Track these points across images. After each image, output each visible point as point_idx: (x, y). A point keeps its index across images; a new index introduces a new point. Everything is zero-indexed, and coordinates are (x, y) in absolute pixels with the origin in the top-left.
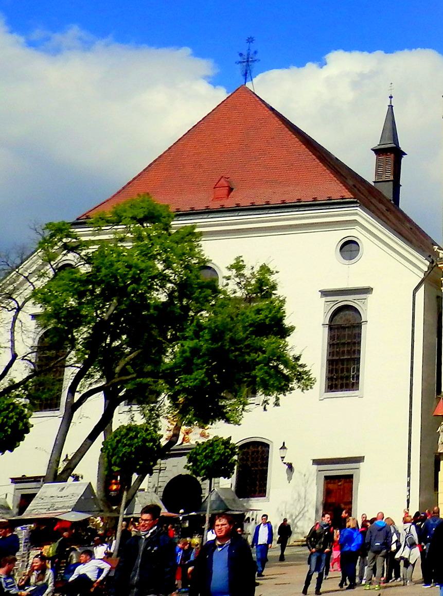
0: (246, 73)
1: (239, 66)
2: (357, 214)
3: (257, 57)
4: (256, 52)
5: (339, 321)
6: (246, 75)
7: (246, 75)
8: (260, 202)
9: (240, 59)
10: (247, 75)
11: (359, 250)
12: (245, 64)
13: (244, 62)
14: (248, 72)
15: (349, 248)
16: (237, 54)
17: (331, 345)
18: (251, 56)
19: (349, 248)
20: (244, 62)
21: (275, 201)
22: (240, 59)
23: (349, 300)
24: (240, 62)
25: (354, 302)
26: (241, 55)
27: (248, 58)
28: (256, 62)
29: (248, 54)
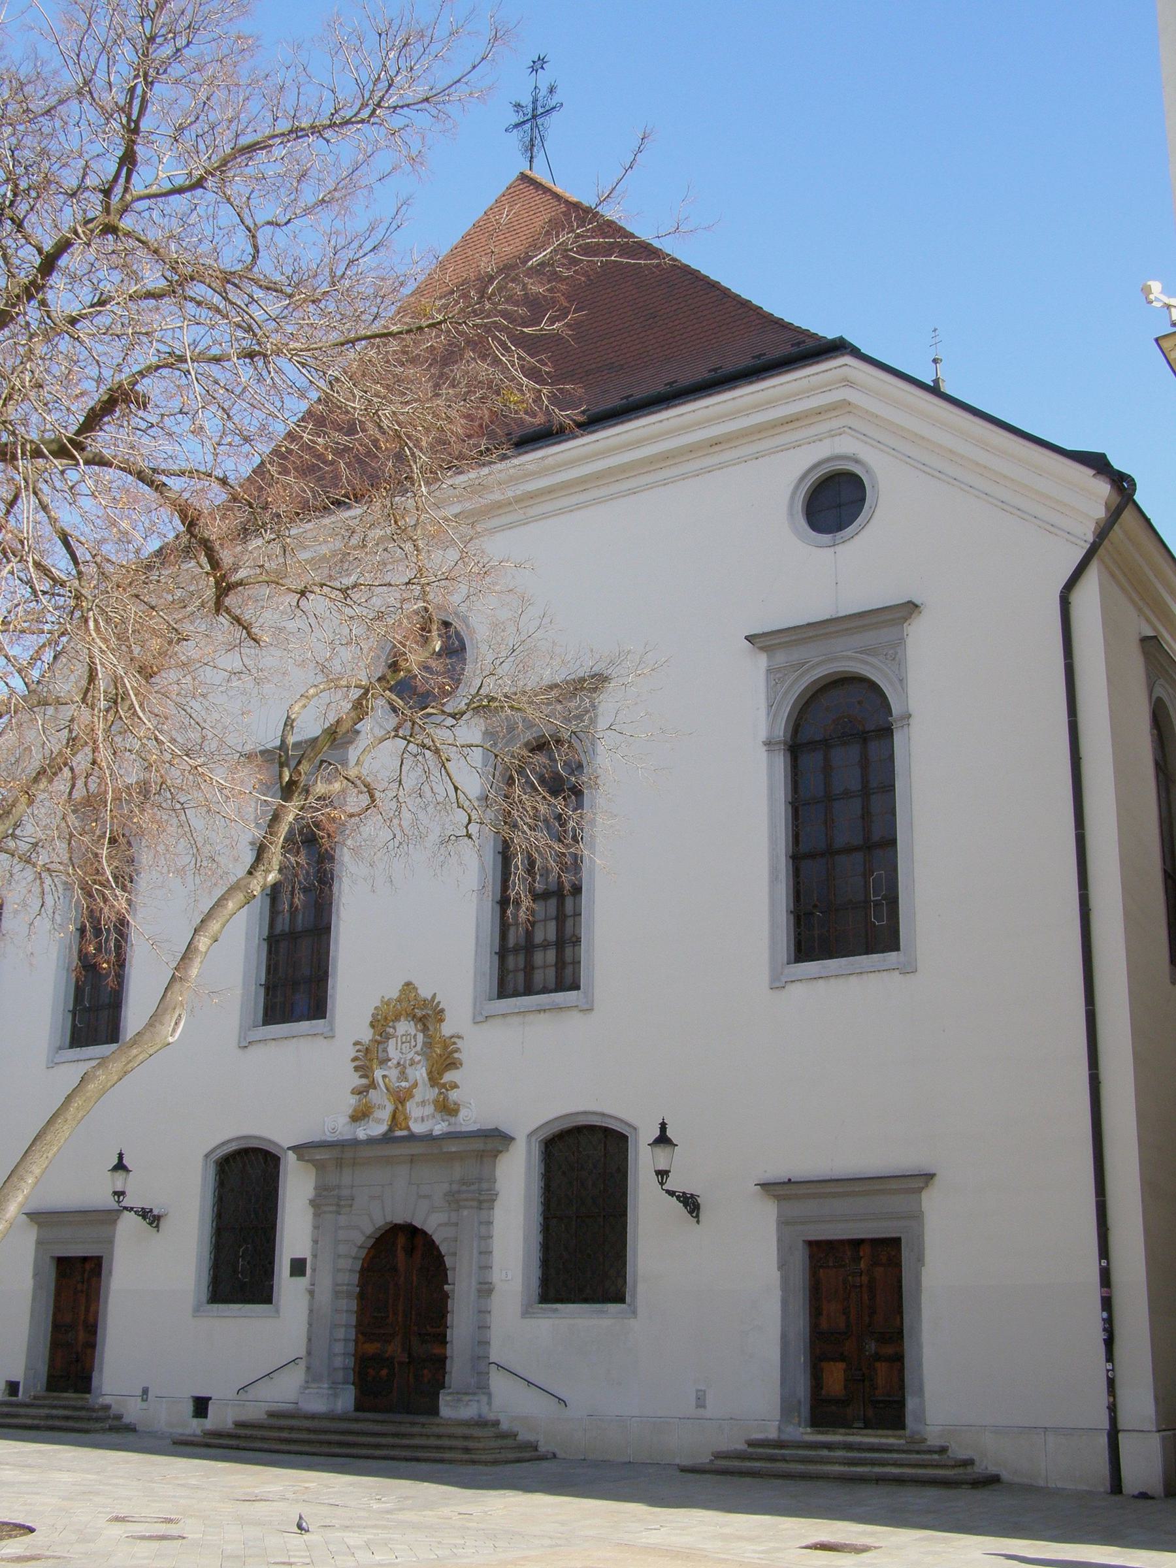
0: (533, 145)
4: (552, 90)
6: (531, 150)
10: (535, 149)
11: (863, 500)
12: (528, 126)
13: (524, 123)
14: (537, 142)
18: (539, 104)
20: (524, 123)
22: (515, 119)
24: (517, 126)
26: (518, 106)
28: (554, 113)
29: (535, 101)
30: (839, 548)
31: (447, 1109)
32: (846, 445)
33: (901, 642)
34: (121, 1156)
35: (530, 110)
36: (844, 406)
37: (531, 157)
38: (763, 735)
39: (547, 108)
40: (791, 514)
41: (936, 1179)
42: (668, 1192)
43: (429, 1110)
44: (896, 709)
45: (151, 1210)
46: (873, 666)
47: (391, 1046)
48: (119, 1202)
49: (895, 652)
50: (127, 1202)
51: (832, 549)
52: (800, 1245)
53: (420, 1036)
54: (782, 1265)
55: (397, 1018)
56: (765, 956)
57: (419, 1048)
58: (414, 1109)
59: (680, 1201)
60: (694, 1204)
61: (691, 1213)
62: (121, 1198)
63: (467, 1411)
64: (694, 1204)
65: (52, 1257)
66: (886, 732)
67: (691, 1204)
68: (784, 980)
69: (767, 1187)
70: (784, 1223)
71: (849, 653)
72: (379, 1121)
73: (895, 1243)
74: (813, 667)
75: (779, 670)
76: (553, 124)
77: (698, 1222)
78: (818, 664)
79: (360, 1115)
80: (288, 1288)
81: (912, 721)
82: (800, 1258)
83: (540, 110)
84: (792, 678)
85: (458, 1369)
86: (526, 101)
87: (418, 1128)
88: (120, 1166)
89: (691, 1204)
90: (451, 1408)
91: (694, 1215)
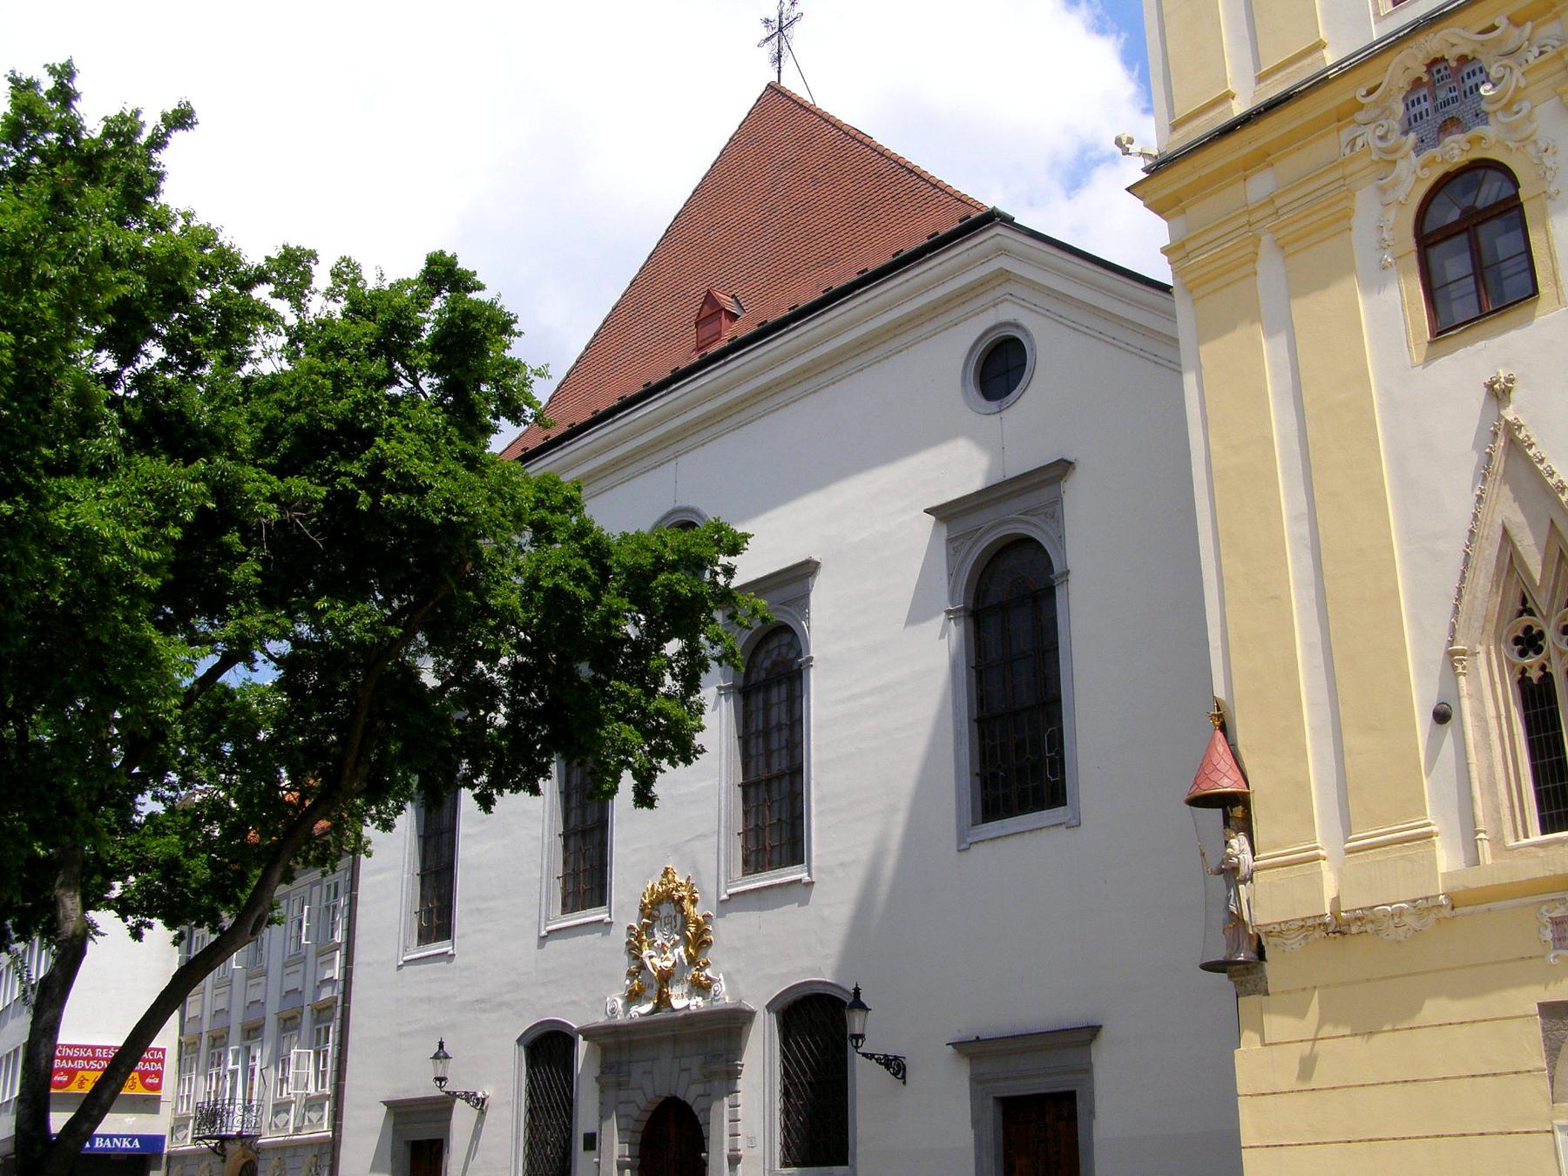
2: (1002, 251)
12: (776, 38)
13: (772, 36)
14: (785, 48)
18: (784, 16)
20: (772, 36)
22: (765, 33)
23: (1010, 522)
24: (767, 39)
25: (1027, 522)
26: (767, 21)
27: (780, 22)
29: (781, 14)
30: (1004, 414)
31: (701, 988)
32: (1008, 313)
33: (1058, 501)
34: (441, 1045)
35: (776, 24)
36: (1004, 276)
37: (780, 68)
39: (791, 19)
40: (964, 384)
41: (1103, 1032)
42: (865, 1055)
43: (686, 987)
44: (1057, 569)
45: (475, 1094)
46: (1035, 526)
48: (440, 1087)
49: (1053, 512)
50: (449, 1087)
51: (998, 416)
52: (991, 1102)
53: (679, 916)
54: (976, 1123)
56: (952, 820)
57: (678, 927)
59: (881, 1064)
60: (898, 1065)
61: (895, 1074)
62: (443, 1083)
64: (898, 1065)
65: (406, 1142)
66: (1048, 593)
67: (895, 1066)
68: (969, 840)
69: (960, 1046)
70: (976, 1080)
71: (1014, 516)
72: (649, 1000)
73: (1070, 1097)
74: (987, 531)
75: (956, 539)
76: (796, 34)
77: (904, 1083)
78: (992, 528)
79: (633, 997)
81: (1070, 577)
82: (992, 1114)
83: (785, 22)
84: (970, 543)
86: (774, 16)
88: (441, 1055)
89: (895, 1066)
91: (899, 1076)
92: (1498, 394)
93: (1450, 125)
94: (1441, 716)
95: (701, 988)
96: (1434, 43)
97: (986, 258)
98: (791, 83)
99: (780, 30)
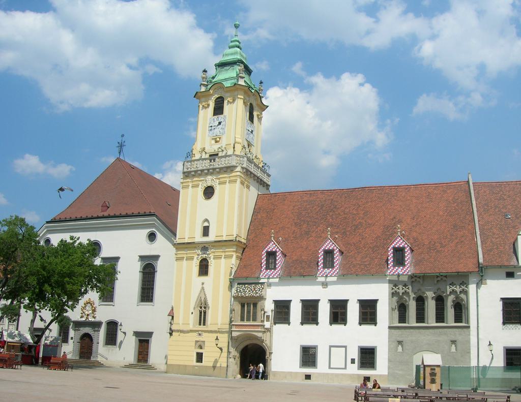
1: (118, 148)
2: (155, 220)
3: (125, 144)
5: (147, 270)
7: (120, 153)
8: (117, 214)
9: (118, 145)
15: (152, 237)
16: (117, 142)
17: (153, 281)
19: (152, 237)
21: (124, 213)
22: (118, 145)
26: (119, 143)
28: (124, 147)
31: (94, 317)
38: (139, 270)
47: (87, 307)
55: (87, 303)
58: (89, 317)
63: (94, 360)
67: (125, 333)
76: (124, 148)
79: (82, 317)
80: (71, 341)
85: (93, 354)
86: (120, 142)
87: (90, 320)
89: (125, 333)
90: (92, 359)
92: (203, 284)
93: (204, 253)
94: (192, 313)
95: (94, 317)
96: (205, 245)
97: (152, 221)
98: (121, 157)
99: (121, 146)
